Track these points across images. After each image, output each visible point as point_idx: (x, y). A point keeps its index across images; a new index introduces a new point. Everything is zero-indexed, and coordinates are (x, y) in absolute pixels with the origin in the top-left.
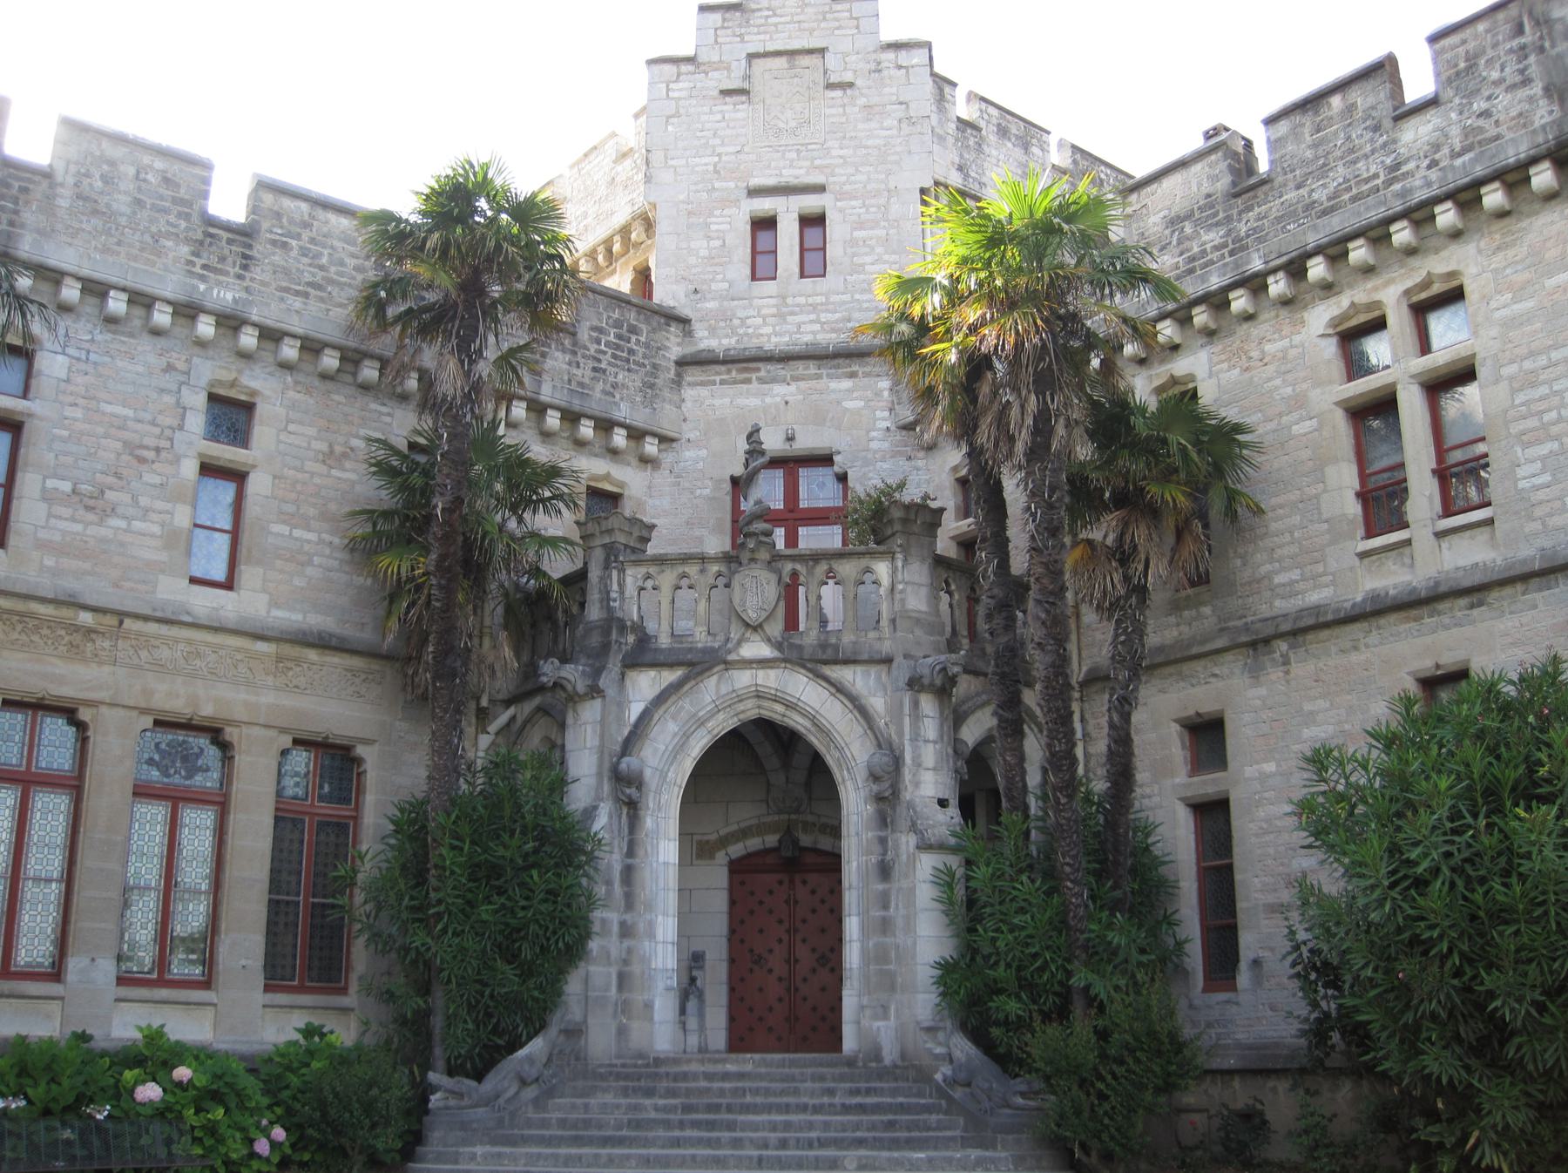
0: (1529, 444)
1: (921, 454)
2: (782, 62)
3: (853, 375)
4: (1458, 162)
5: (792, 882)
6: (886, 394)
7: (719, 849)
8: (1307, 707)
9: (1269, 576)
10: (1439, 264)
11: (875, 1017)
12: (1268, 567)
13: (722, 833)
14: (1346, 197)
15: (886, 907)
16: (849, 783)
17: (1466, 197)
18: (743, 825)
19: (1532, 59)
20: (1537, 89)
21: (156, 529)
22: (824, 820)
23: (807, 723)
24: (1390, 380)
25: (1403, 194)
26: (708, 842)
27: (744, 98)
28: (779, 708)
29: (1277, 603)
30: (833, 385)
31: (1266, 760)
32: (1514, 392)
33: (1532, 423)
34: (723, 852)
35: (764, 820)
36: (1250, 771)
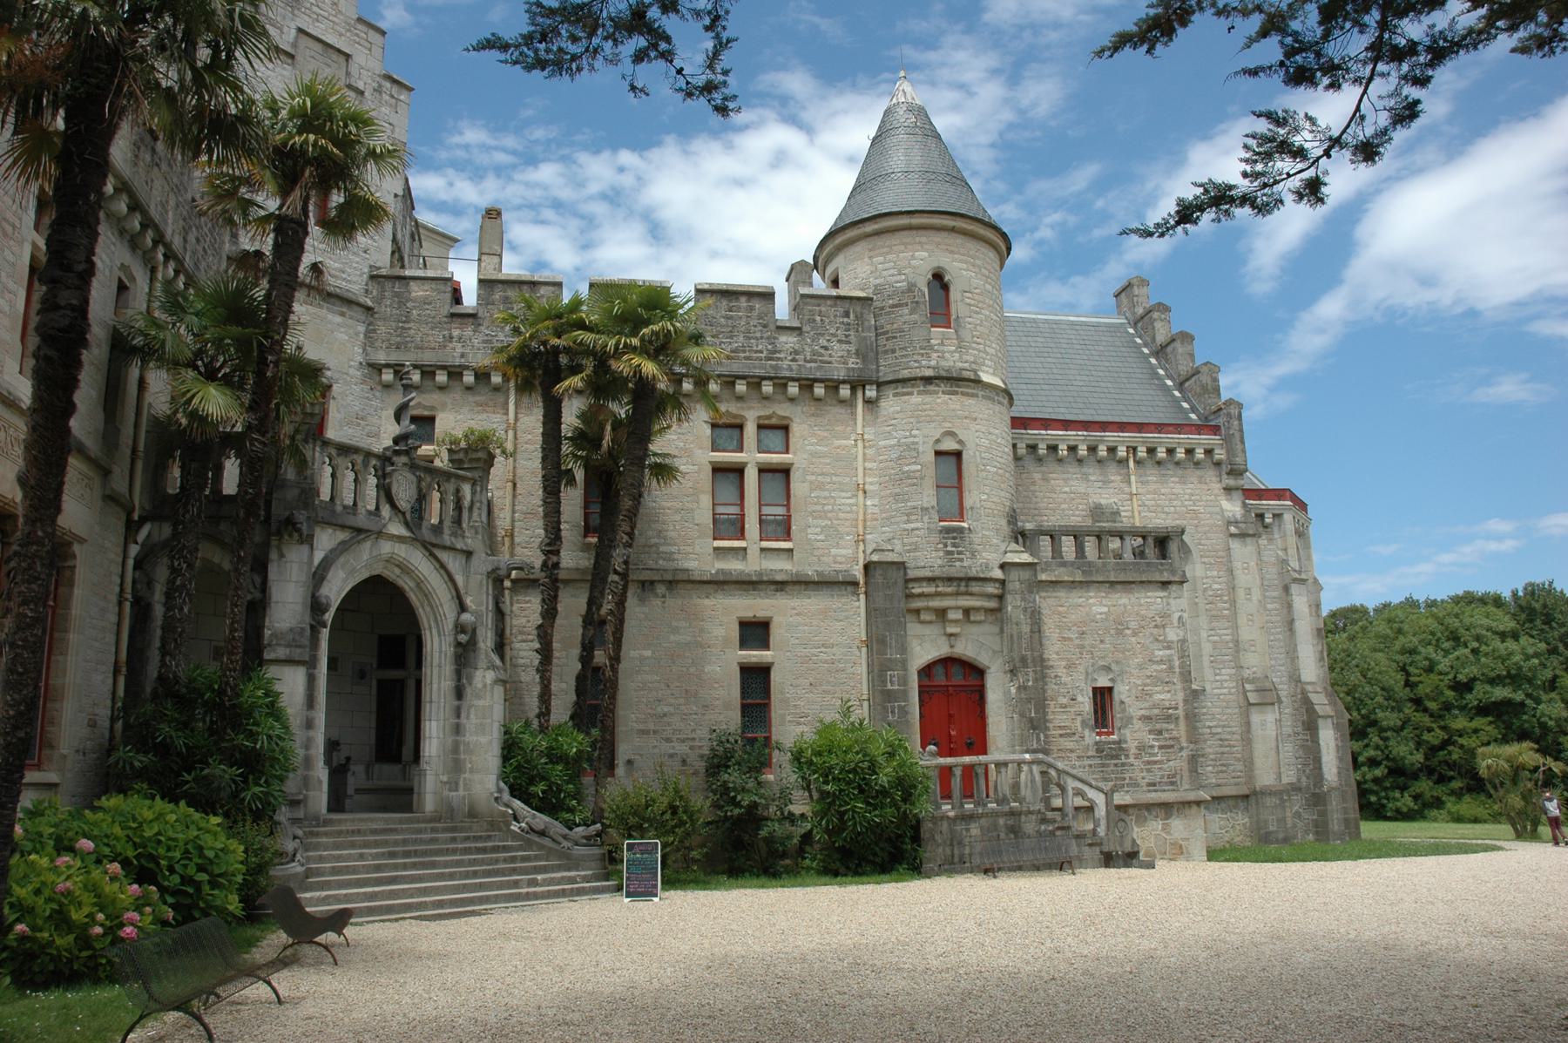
0: (816, 518)
1: (379, 388)
2: (318, 47)
3: (342, 314)
4: (808, 365)
6: (362, 336)
8: (675, 624)
9: (656, 545)
10: (782, 410)
11: (450, 790)
12: (656, 540)
14: (742, 355)
15: (458, 716)
16: (434, 631)
17: (807, 385)
19: (852, 333)
20: (853, 348)
21: (7, 309)
23: (412, 584)
24: (744, 460)
25: (775, 368)
27: (290, 61)
28: (397, 571)
29: (661, 562)
30: (330, 316)
31: (644, 649)
32: (812, 490)
33: (819, 508)
36: (633, 653)
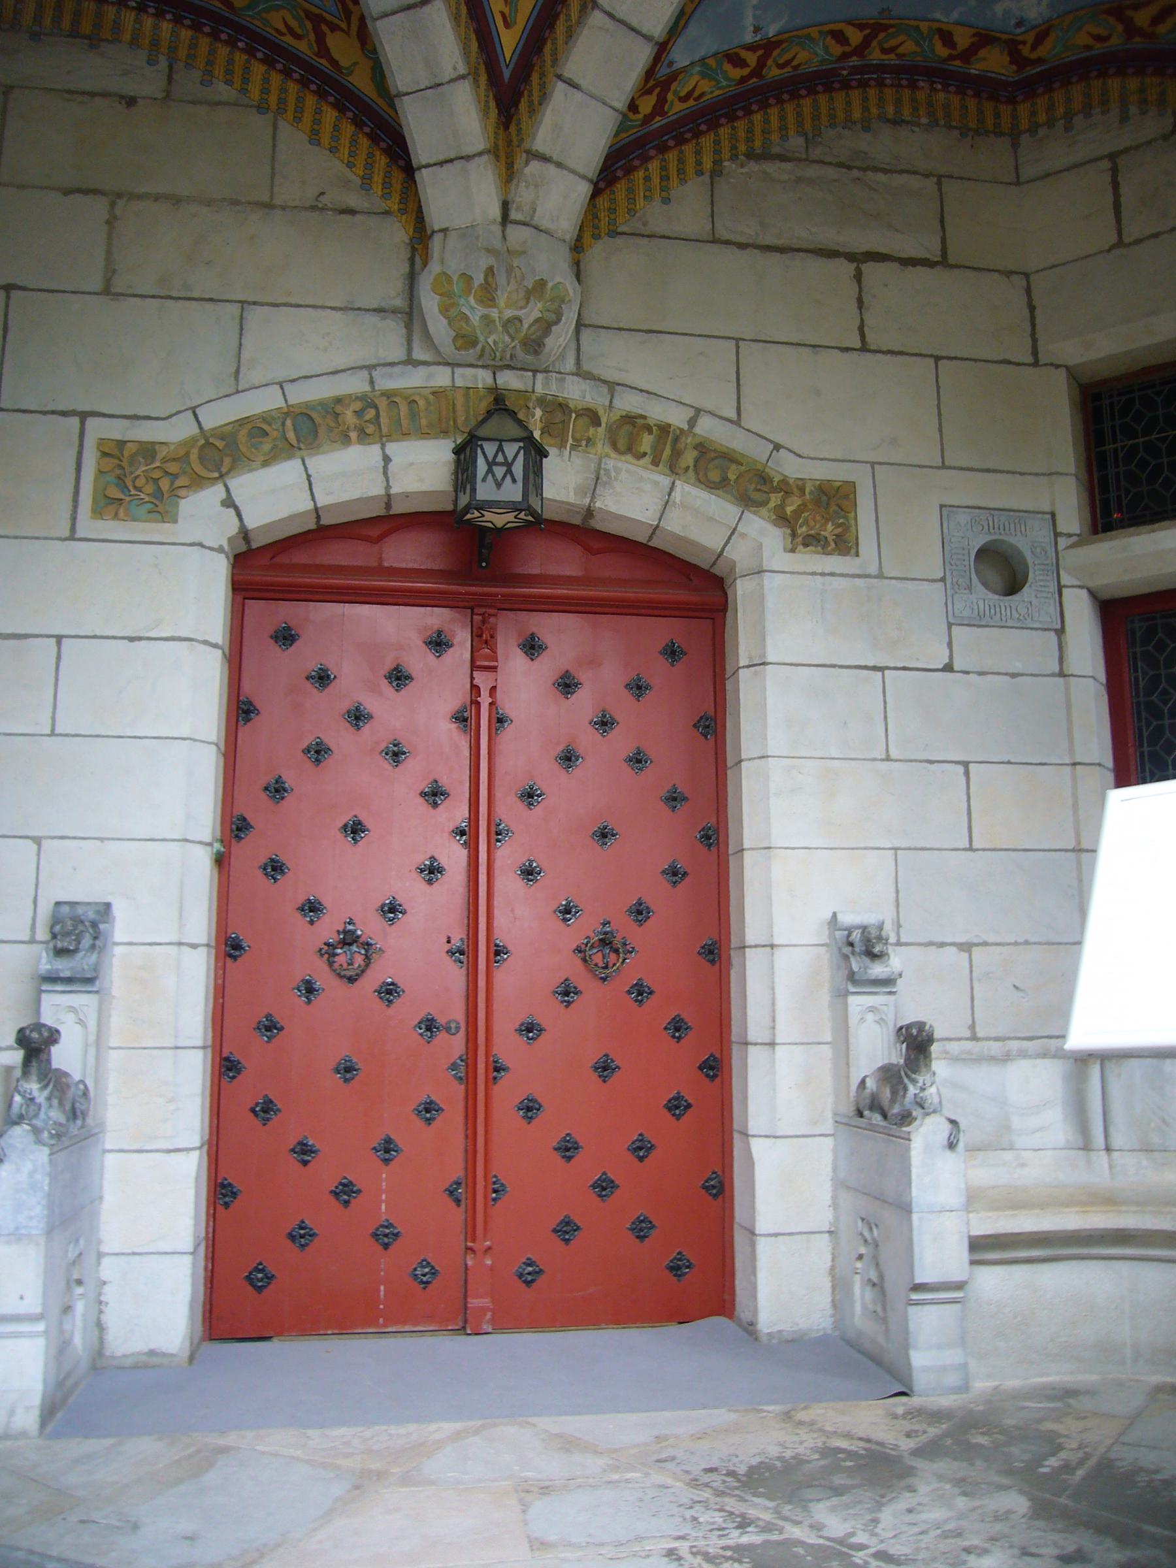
5: (483, 640)
7: (198, 482)
13: (216, 416)
18: (301, 394)
22: (628, 403)
26: (148, 450)
34: (213, 494)
35: (388, 382)
